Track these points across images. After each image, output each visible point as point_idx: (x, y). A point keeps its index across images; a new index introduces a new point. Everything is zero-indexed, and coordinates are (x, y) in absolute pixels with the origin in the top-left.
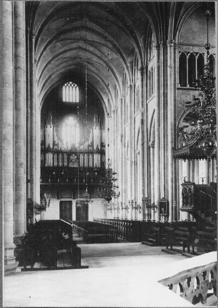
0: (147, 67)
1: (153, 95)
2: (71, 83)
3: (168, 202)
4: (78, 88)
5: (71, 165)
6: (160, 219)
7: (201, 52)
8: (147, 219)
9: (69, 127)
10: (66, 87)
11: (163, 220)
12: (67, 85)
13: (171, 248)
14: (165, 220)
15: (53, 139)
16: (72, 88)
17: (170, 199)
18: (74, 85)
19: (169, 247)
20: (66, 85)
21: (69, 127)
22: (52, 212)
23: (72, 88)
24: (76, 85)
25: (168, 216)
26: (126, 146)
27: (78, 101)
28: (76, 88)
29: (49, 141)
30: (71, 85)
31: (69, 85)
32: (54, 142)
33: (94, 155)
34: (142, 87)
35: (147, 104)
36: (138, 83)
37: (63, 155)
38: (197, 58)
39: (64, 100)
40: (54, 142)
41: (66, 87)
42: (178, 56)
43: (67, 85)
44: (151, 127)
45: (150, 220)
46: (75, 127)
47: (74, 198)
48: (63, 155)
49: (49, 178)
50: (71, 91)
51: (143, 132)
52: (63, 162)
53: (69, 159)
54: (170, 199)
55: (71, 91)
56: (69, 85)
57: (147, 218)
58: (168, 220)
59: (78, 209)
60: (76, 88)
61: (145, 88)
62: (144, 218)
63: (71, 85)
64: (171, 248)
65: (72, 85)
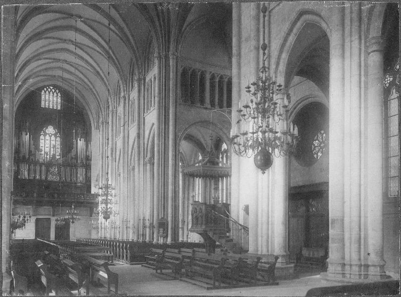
0: (145, 79)
1: (152, 109)
2: (51, 88)
3: (168, 222)
4: (59, 94)
5: (50, 178)
6: (158, 240)
7: (204, 69)
8: (141, 240)
9: (48, 136)
10: (45, 92)
11: (161, 241)
12: (47, 90)
13: (161, 271)
14: (164, 240)
15: (30, 148)
17: (170, 219)
18: (55, 91)
19: (159, 271)
20: (45, 89)
21: (48, 136)
22: (27, 233)
24: (57, 91)
25: (167, 236)
26: (117, 160)
27: (59, 108)
28: (57, 94)
29: (25, 151)
30: (51, 90)
32: (30, 152)
33: (79, 169)
34: (139, 100)
35: (144, 118)
36: (134, 94)
37: (41, 166)
38: (199, 73)
39: (43, 106)
40: (30, 152)
41: (45, 92)
42: (180, 70)
43: (47, 90)
44: (148, 142)
45: (145, 242)
46: (56, 137)
47: (54, 216)
48: (41, 166)
49: (34, 192)
50: (51, 97)
51: (139, 147)
52: (40, 175)
53: (47, 171)
54: (170, 219)
55: (51, 97)
56: (49, 90)
57: (141, 238)
58: (167, 241)
59: (57, 228)
61: (142, 98)
62: (138, 238)
63: (51, 90)
64: (161, 271)
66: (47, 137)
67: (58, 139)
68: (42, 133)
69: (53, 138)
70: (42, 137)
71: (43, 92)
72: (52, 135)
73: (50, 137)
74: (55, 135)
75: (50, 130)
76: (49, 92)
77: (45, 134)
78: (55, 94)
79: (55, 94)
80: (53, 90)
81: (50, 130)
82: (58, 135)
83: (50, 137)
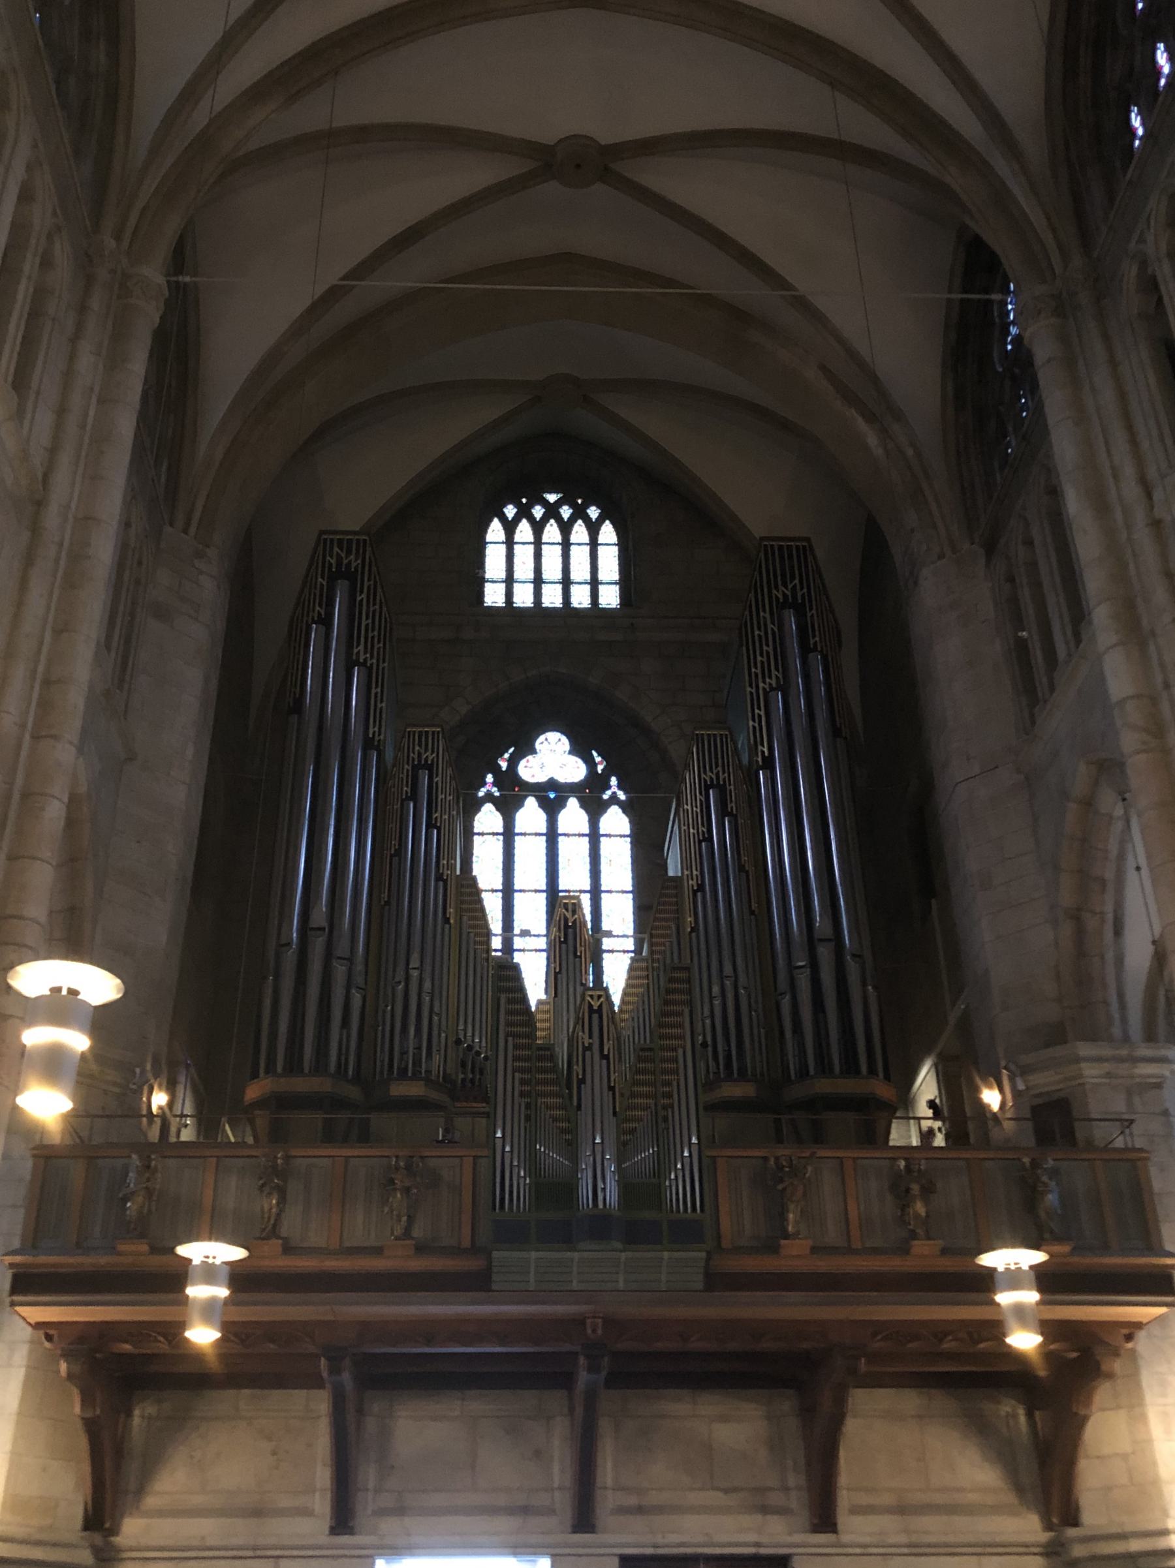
2: (552, 498)
4: (608, 533)
9: (531, 803)
10: (510, 528)
16: (566, 529)
20: (510, 511)
21: (531, 803)
23: (566, 529)
24: (593, 512)
28: (593, 529)
31: (538, 512)
39: (494, 596)
41: (510, 528)
46: (595, 808)
56: (538, 512)
60: (593, 529)
65: (566, 512)
66: (530, 815)
67: (615, 821)
69: (573, 816)
70: (488, 819)
71: (495, 531)
73: (552, 808)
76: (538, 528)
78: (580, 532)
79: (580, 532)
80: (566, 512)
83: (552, 808)
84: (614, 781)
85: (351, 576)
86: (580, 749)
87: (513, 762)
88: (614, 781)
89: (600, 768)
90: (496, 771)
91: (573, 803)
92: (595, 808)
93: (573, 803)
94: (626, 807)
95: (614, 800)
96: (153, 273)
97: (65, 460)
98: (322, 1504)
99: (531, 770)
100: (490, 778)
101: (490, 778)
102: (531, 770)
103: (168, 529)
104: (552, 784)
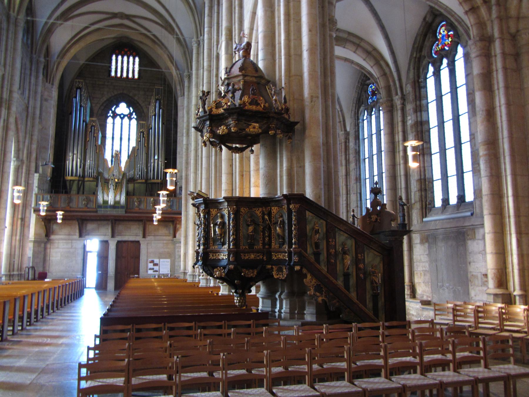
2: (126, 50)
21: (118, 117)
46: (130, 119)
66: (118, 119)
67: (134, 122)
68: (110, 113)
69: (126, 119)
70: (110, 120)
72: (125, 116)
73: (122, 119)
74: (130, 117)
75: (123, 108)
77: (115, 115)
81: (123, 108)
82: (134, 116)
83: (122, 119)
84: (134, 114)
85: (80, 88)
86: (128, 107)
87: (115, 109)
88: (134, 114)
89: (131, 112)
90: (112, 110)
91: (126, 118)
92: (130, 119)
93: (126, 118)
94: (136, 119)
95: (134, 118)
96: (42, 59)
97: (31, 99)
98: (78, 234)
99: (119, 111)
100: (110, 112)
101: (110, 112)
102: (119, 111)
103: (46, 84)
104: (122, 114)
